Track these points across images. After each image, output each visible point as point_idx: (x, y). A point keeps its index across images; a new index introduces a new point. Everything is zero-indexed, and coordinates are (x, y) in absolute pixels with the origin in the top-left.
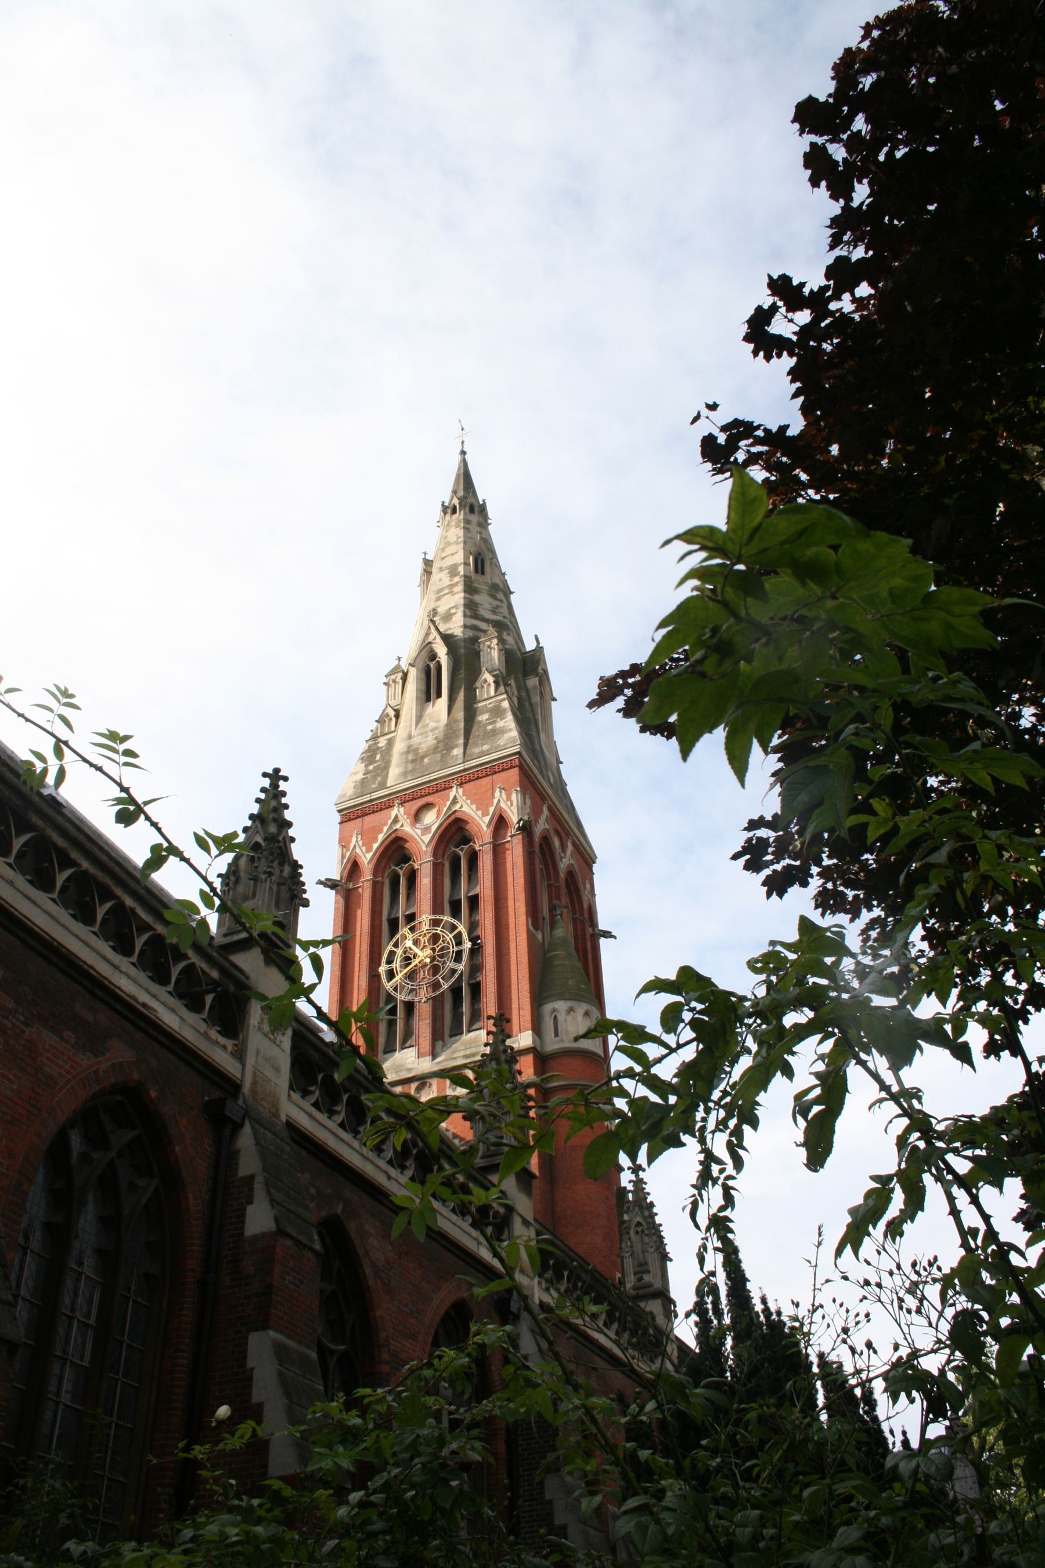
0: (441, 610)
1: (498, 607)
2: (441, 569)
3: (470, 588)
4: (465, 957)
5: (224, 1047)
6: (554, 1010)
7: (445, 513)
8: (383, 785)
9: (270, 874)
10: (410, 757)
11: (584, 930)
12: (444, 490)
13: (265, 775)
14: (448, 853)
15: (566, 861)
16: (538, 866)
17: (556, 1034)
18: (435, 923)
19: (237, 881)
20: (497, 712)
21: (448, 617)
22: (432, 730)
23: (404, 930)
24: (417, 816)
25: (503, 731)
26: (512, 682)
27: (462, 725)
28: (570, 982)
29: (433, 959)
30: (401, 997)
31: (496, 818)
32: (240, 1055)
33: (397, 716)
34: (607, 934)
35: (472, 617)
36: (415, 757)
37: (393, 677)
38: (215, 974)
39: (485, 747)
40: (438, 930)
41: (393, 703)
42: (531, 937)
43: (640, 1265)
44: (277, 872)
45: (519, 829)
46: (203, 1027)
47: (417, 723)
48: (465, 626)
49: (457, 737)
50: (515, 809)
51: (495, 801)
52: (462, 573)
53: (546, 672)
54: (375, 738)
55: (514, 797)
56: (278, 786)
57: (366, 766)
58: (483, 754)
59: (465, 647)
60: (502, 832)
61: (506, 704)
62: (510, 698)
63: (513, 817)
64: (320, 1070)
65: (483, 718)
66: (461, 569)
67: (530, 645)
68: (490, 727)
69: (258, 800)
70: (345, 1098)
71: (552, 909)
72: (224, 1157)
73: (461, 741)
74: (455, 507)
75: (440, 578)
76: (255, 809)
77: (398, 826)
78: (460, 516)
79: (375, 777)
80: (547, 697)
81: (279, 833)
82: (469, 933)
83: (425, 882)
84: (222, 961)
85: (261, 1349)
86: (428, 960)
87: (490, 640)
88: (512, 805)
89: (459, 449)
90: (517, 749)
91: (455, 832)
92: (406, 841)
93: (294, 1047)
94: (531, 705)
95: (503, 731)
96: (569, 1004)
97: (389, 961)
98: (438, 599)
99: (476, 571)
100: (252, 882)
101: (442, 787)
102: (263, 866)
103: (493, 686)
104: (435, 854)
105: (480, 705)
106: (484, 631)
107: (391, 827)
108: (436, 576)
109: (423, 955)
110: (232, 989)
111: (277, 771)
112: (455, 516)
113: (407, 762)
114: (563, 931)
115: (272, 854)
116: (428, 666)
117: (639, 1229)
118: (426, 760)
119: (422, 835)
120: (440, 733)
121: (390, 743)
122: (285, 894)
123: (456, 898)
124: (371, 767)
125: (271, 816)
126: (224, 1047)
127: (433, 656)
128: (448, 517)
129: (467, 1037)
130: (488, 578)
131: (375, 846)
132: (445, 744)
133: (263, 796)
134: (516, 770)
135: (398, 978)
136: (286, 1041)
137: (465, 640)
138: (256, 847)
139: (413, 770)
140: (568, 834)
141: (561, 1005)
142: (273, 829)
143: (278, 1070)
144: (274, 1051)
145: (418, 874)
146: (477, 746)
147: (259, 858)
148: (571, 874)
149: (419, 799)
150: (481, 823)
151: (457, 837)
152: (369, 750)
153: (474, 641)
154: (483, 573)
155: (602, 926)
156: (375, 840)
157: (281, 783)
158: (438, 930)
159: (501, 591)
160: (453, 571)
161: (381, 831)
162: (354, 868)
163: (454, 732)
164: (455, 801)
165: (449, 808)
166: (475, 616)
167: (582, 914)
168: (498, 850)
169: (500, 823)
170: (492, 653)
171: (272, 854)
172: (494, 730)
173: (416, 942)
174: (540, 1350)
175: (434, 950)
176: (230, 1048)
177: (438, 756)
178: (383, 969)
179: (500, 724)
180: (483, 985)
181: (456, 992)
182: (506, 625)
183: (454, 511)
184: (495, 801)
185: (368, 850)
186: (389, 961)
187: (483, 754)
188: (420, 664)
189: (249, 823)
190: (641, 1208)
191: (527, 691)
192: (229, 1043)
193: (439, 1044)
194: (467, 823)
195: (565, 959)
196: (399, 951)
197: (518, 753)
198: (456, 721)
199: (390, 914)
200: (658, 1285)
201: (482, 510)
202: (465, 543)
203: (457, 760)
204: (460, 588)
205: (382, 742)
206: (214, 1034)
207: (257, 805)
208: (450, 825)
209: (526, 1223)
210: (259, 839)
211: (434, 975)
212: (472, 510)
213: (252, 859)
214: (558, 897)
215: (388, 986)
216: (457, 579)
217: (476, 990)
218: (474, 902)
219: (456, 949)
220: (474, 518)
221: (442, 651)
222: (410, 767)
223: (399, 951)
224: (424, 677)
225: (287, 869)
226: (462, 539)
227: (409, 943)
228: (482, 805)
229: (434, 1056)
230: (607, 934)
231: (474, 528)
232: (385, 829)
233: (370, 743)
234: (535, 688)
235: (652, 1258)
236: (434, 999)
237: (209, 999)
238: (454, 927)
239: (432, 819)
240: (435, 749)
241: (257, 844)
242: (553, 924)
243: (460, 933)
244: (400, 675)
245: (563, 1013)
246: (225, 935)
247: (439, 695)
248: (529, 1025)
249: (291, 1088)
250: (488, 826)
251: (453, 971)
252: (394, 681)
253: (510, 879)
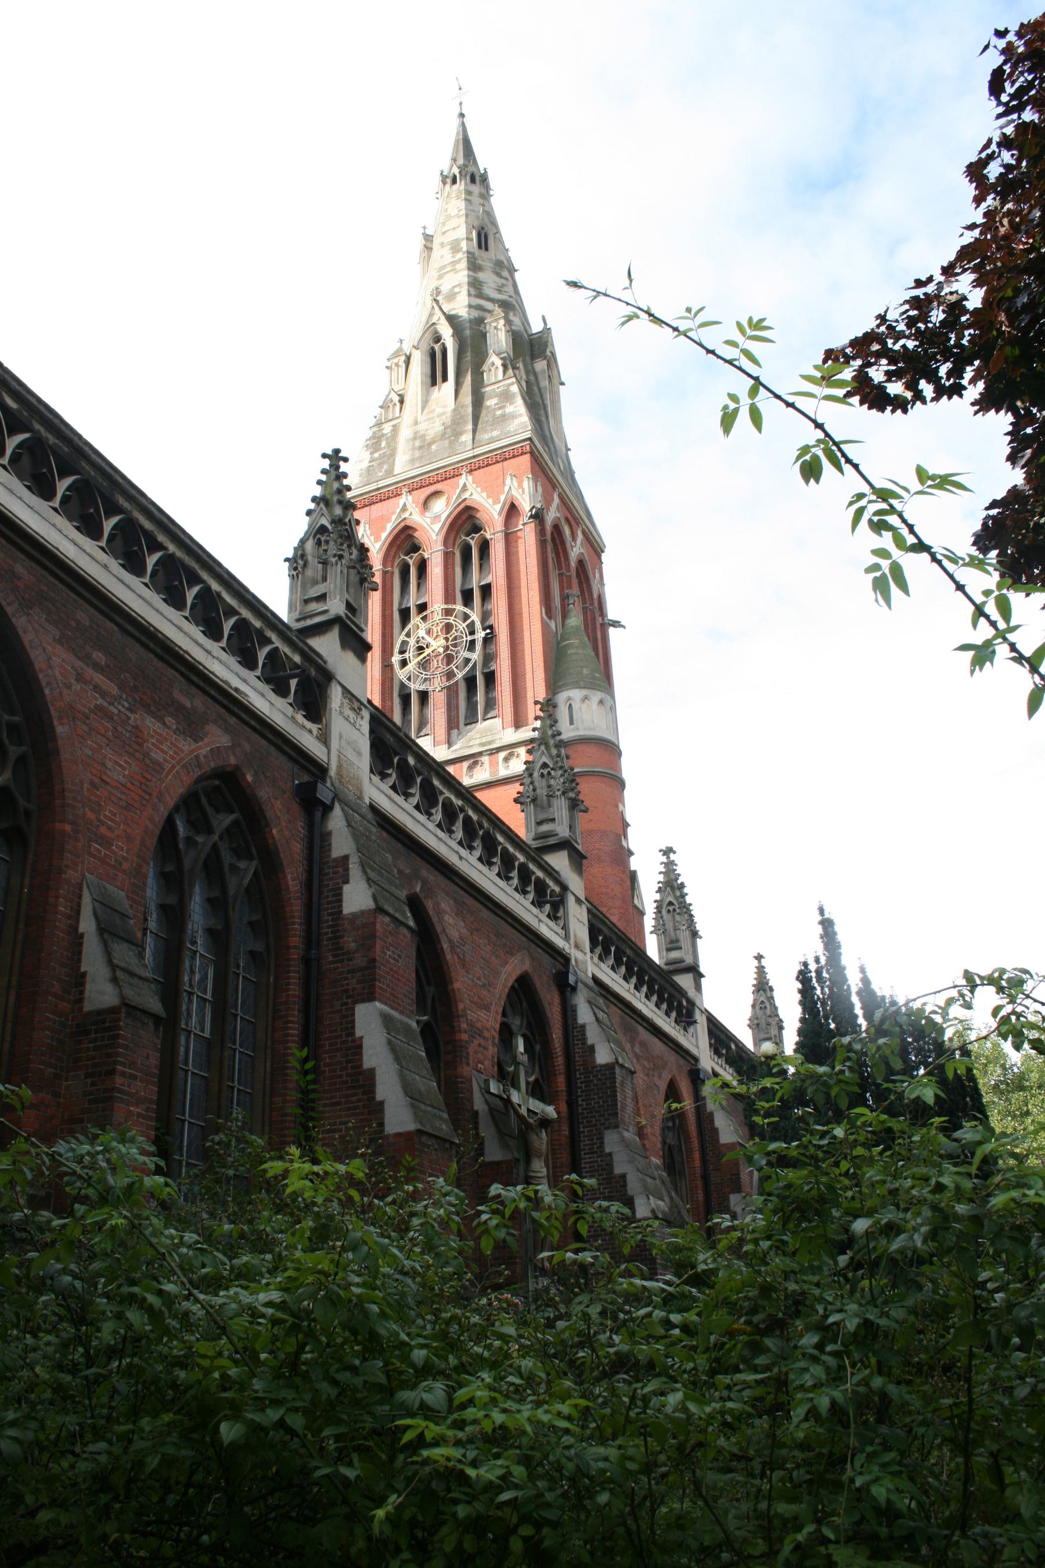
0: (445, 289)
1: (503, 285)
2: (442, 245)
3: (474, 266)
4: (479, 646)
5: (310, 731)
6: (569, 699)
7: (444, 183)
8: (390, 473)
9: (341, 557)
10: (417, 444)
11: (594, 619)
12: (443, 157)
13: (324, 456)
14: (458, 541)
15: (576, 550)
16: (550, 555)
17: (572, 723)
18: (448, 612)
19: (305, 565)
20: (506, 397)
21: (452, 296)
22: (439, 416)
23: (415, 619)
24: (426, 504)
25: (513, 416)
26: (520, 365)
27: (470, 410)
28: (585, 671)
29: (447, 648)
30: (414, 687)
31: (507, 506)
32: (324, 738)
33: (402, 402)
34: (616, 624)
35: (476, 296)
36: (422, 444)
37: (396, 360)
38: (297, 659)
39: (495, 433)
40: (451, 620)
41: (396, 388)
42: (545, 627)
43: (672, 942)
44: (346, 554)
45: (531, 517)
46: (290, 711)
47: (423, 408)
48: (470, 306)
49: (466, 422)
50: (526, 497)
51: (506, 489)
52: (465, 249)
53: (553, 354)
54: (379, 424)
55: (525, 484)
56: (338, 467)
57: (372, 453)
58: (492, 440)
59: (471, 328)
60: (514, 520)
61: (515, 389)
62: (519, 382)
63: (526, 505)
64: (397, 754)
65: (491, 403)
66: (464, 245)
67: (536, 327)
68: (499, 413)
69: (319, 482)
70: (419, 780)
71: (564, 598)
72: (317, 840)
73: (470, 427)
74: (455, 177)
75: (442, 255)
76: (318, 491)
77: (406, 515)
78: (461, 186)
79: (381, 465)
80: (555, 381)
81: (345, 515)
82: (484, 620)
83: (436, 571)
84: (301, 644)
85: (368, 1020)
86: (441, 650)
87: (496, 320)
88: (525, 494)
89: (458, 111)
90: (528, 435)
91: (466, 521)
92: (415, 530)
93: (372, 731)
94: (540, 389)
95: (513, 416)
96: (584, 692)
97: (402, 652)
98: (440, 277)
99: (480, 247)
100: (320, 566)
101: (451, 474)
102: (332, 549)
103: (501, 369)
104: (445, 543)
105: (488, 389)
106: (489, 312)
107: (399, 515)
108: (436, 252)
109: (437, 644)
110: (313, 673)
111: (337, 451)
112: (455, 187)
113: (414, 449)
114: (575, 620)
115: (341, 537)
116: (433, 349)
117: (671, 908)
118: (434, 447)
119: (432, 526)
120: (447, 418)
121: (395, 429)
122: (354, 578)
123: (467, 587)
124: (376, 455)
125: (335, 498)
126: (310, 731)
127: (438, 339)
128: (448, 186)
129: (481, 726)
130: (492, 253)
131: (384, 535)
132: (453, 430)
133: (324, 478)
134: (528, 456)
135: (411, 666)
136: (365, 726)
137: (470, 321)
138: (323, 529)
139: (421, 457)
140: (578, 524)
141: (576, 694)
142: (338, 511)
143: (359, 754)
144: (355, 735)
145: (429, 564)
146: (486, 431)
147: (327, 542)
148: (581, 563)
149: (428, 486)
150: (492, 513)
151: (468, 526)
152: (373, 437)
153: (480, 321)
154: (487, 249)
155: (612, 614)
156: (383, 529)
157: (341, 463)
158: (451, 620)
159: (505, 268)
160: (455, 248)
161: (389, 520)
163: (462, 417)
164: (464, 488)
165: (459, 496)
166: (480, 295)
167: (592, 604)
168: (510, 538)
169: (512, 510)
170: (498, 337)
171: (341, 537)
172: (503, 416)
173: (429, 632)
174: (597, 1019)
175: (447, 639)
176: (315, 732)
177: (447, 442)
178: (396, 659)
179: (510, 409)
180: (497, 675)
181: (470, 681)
182: (511, 306)
183: (454, 181)
184: (506, 489)
185: (377, 540)
186: (402, 652)
187: (492, 440)
188: (425, 347)
189: (312, 506)
190: (672, 888)
191: (535, 375)
192: (314, 727)
193: (455, 732)
194: (477, 510)
195: (578, 647)
196: (412, 641)
197: (530, 439)
198: (463, 406)
199: (400, 604)
200: (689, 960)
201: (484, 179)
202: (467, 216)
203: (466, 446)
204: (464, 264)
205: (387, 428)
206: (300, 718)
207: (319, 488)
208: (460, 514)
209: (578, 901)
210: (325, 522)
211: (448, 664)
212: (473, 180)
213: (319, 543)
214: (570, 587)
215: (401, 674)
216: (460, 255)
217: (490, 678)
218: (486, 591)
219: (469, 638)
220: (476, 189)
221: (446, 333)
222: (417, 454)
223: (412, 641)
224: (429, 360)
225: (355, 552)
226: (463, 212)
227: (422, 633)
228: (493, 494)
229: (450, 744)
230: (616, 624)
231: (476, 200)
232: (394, 517)
233: (375, 429)
234: (543, 371)
235: (684, 936)
236: (448, 688)
237: (293, 683)
238: (466, 617)
239: (442, 508)
240: (443, 436)
241: (323, 527)
242: (565, 616)
243: (473, 622)
244: (403, 358)
245: (578, 701)
246: (298, 620)
247: (445, 379)
249: (371, 771)
250: (500, 514)
251: (467, 661)
252: (397, 365)
253: (522, 568)
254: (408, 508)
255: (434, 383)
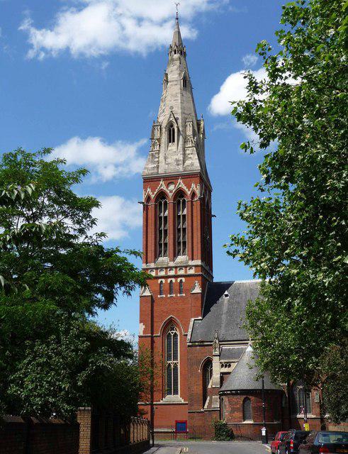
24: (167, 187)
63: (198, 192)
83: (170, 206)
127: (172, 126)
149: (170, 179)
162: (148, 198)
169: (194, 194)
212: (181, 54)
228: (189, 187)
247: (174, 141)
248: (200, 255)
254: (162, 185)
255: (170, 142)
